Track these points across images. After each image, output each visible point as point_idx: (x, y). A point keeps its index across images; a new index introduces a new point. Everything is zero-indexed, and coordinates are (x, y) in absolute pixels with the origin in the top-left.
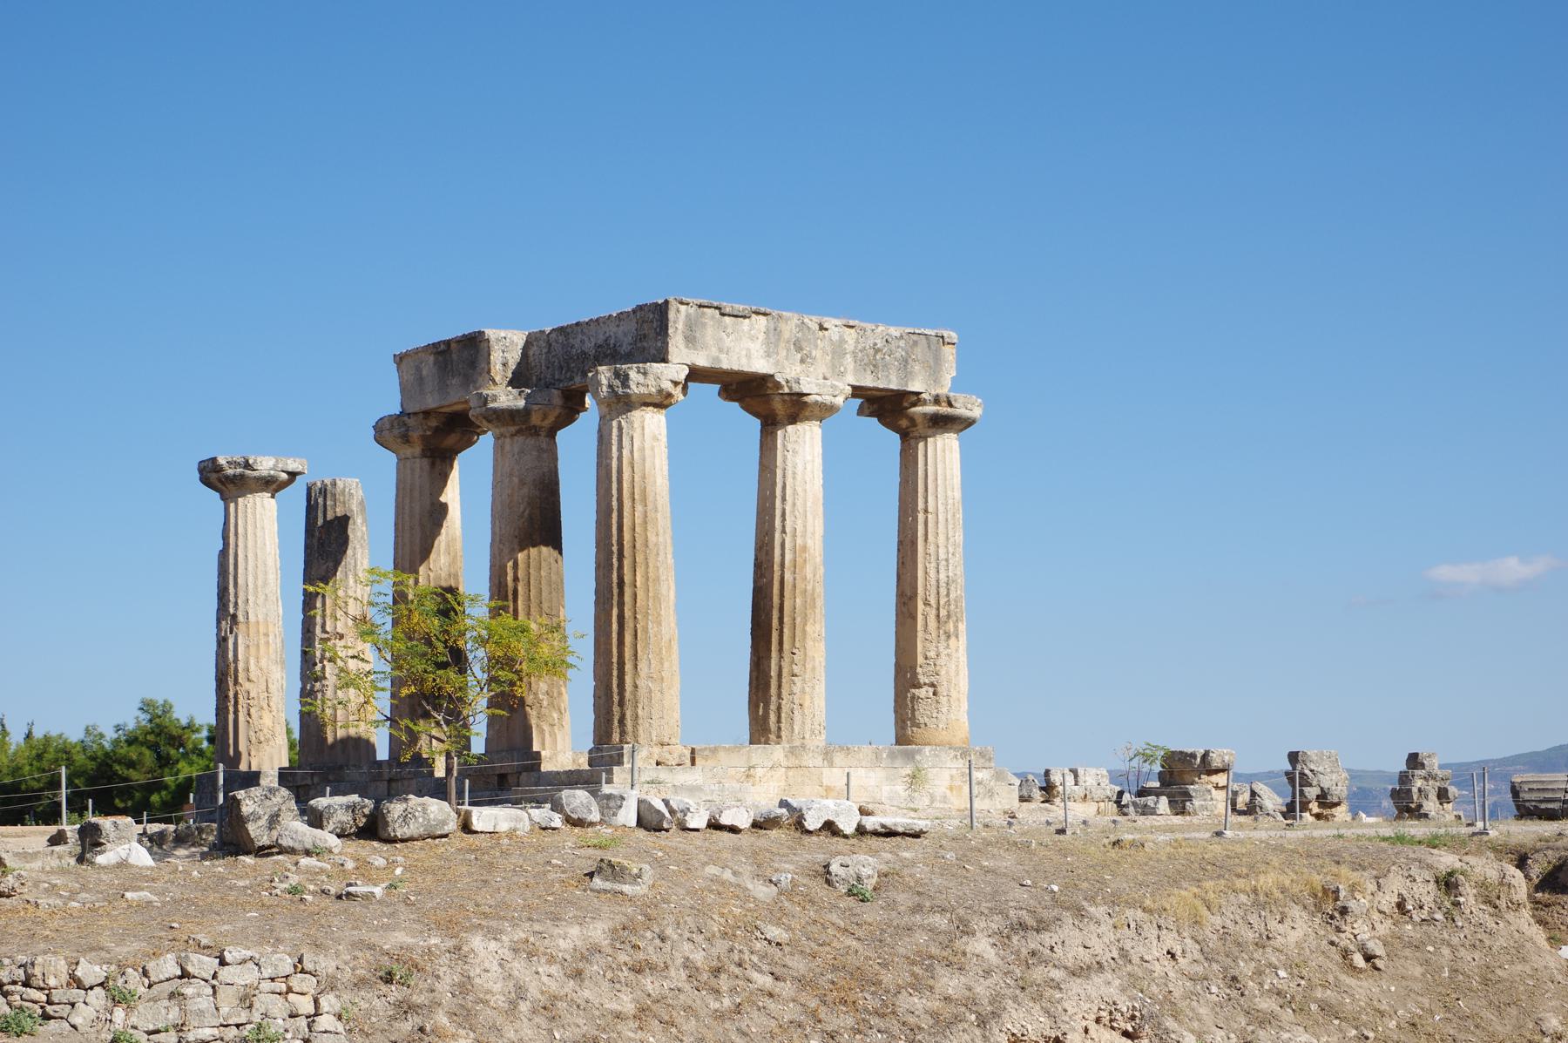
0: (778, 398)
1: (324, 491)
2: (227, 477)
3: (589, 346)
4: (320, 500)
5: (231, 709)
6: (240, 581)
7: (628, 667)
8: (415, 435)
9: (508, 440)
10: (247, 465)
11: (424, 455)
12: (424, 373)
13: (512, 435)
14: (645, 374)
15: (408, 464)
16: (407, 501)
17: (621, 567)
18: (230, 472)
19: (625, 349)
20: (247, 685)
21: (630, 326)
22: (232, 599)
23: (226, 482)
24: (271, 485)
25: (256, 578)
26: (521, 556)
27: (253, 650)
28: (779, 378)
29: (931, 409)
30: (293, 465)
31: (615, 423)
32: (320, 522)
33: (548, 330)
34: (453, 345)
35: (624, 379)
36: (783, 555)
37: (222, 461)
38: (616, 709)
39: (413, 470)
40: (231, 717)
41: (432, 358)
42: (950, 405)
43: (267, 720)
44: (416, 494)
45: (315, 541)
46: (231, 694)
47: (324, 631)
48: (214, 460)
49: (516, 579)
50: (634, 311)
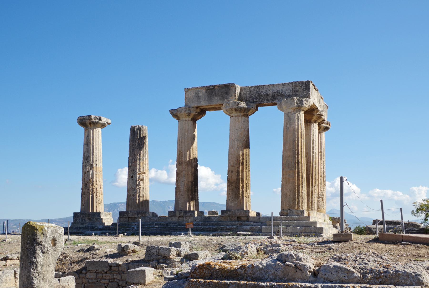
0: (316, 115)
1: (139, 129)
2: (93, 122)
3: (270, 92)
4: (138, 131)
5: (91, 193)
6: (94, 154)
7: (300, 187)
8: (193, 114)
9: (240, 117)
10: (100, 119)
11: (192, 120)
12: (200, 95)
13: (242, 116)
14: (307, 101)
15: (186, 122)
16: (186, 134)
17: (298, 157)
18: (94, 121)
19: (287, 93)
20: (96, 186)
21: (291, 87)
22: (91, 160)
23: (87, 123)
24: (103, 126)
25: (99, 154)
26: (244, 151)
27: (98, 175)
28: (319, 109)
29: (326, 125)
30: (109, 122)
31: (296, 115)
32: (138, 138)
33: (249, 86)
34: (216, 87)
35: (302, 102)
36: (313, 159)
37: (93, 117)
38: (297, 199)
39: (188, 124)
40: (91, 195)
41: (204, 91)
42: (329, 125)
43: (101, 197)
44: (189, 131)
45: (137, 144)
46: (91, 188)
47: (140, 171)
48: (90, 116)
49: (243, 159)
50: (292, 83)
